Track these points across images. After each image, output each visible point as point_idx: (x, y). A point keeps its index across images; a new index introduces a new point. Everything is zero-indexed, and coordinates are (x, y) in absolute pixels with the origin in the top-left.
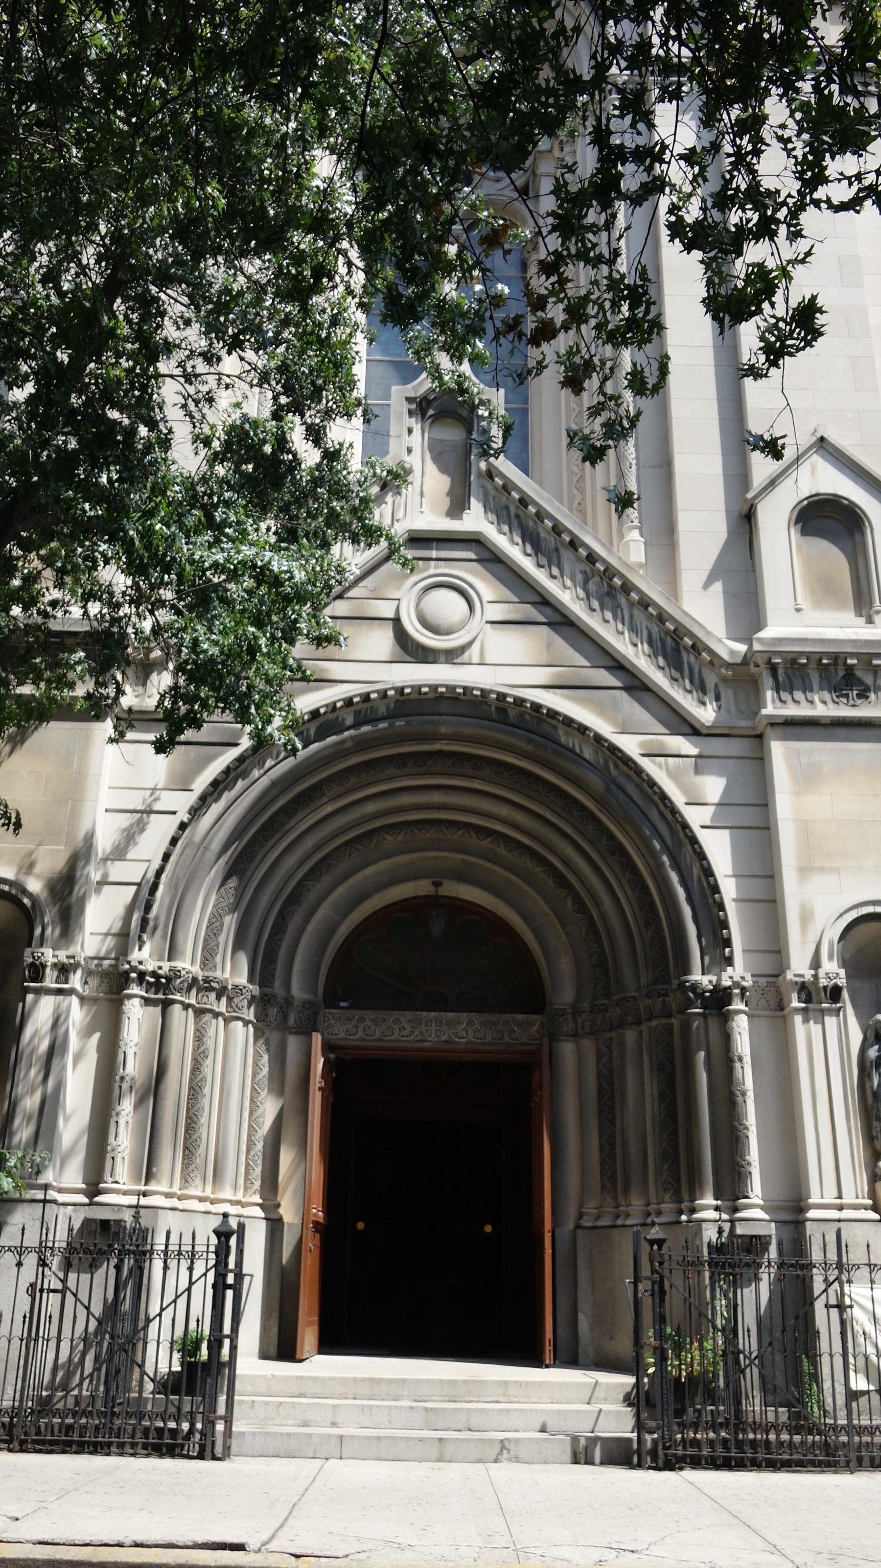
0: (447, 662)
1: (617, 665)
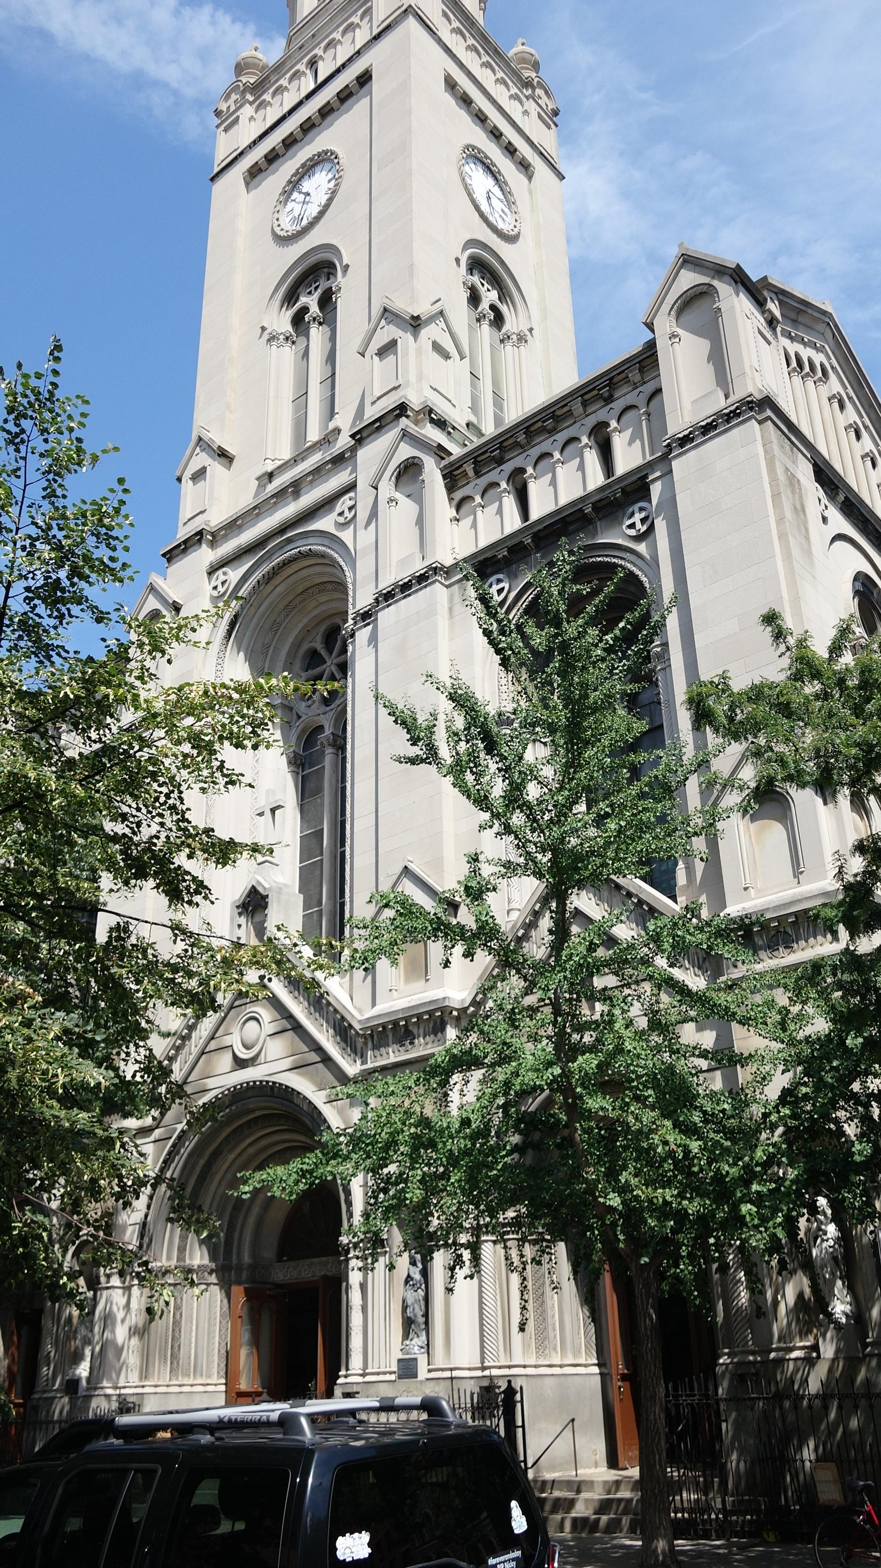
0: (253, 1065)
1: (318, 1049)
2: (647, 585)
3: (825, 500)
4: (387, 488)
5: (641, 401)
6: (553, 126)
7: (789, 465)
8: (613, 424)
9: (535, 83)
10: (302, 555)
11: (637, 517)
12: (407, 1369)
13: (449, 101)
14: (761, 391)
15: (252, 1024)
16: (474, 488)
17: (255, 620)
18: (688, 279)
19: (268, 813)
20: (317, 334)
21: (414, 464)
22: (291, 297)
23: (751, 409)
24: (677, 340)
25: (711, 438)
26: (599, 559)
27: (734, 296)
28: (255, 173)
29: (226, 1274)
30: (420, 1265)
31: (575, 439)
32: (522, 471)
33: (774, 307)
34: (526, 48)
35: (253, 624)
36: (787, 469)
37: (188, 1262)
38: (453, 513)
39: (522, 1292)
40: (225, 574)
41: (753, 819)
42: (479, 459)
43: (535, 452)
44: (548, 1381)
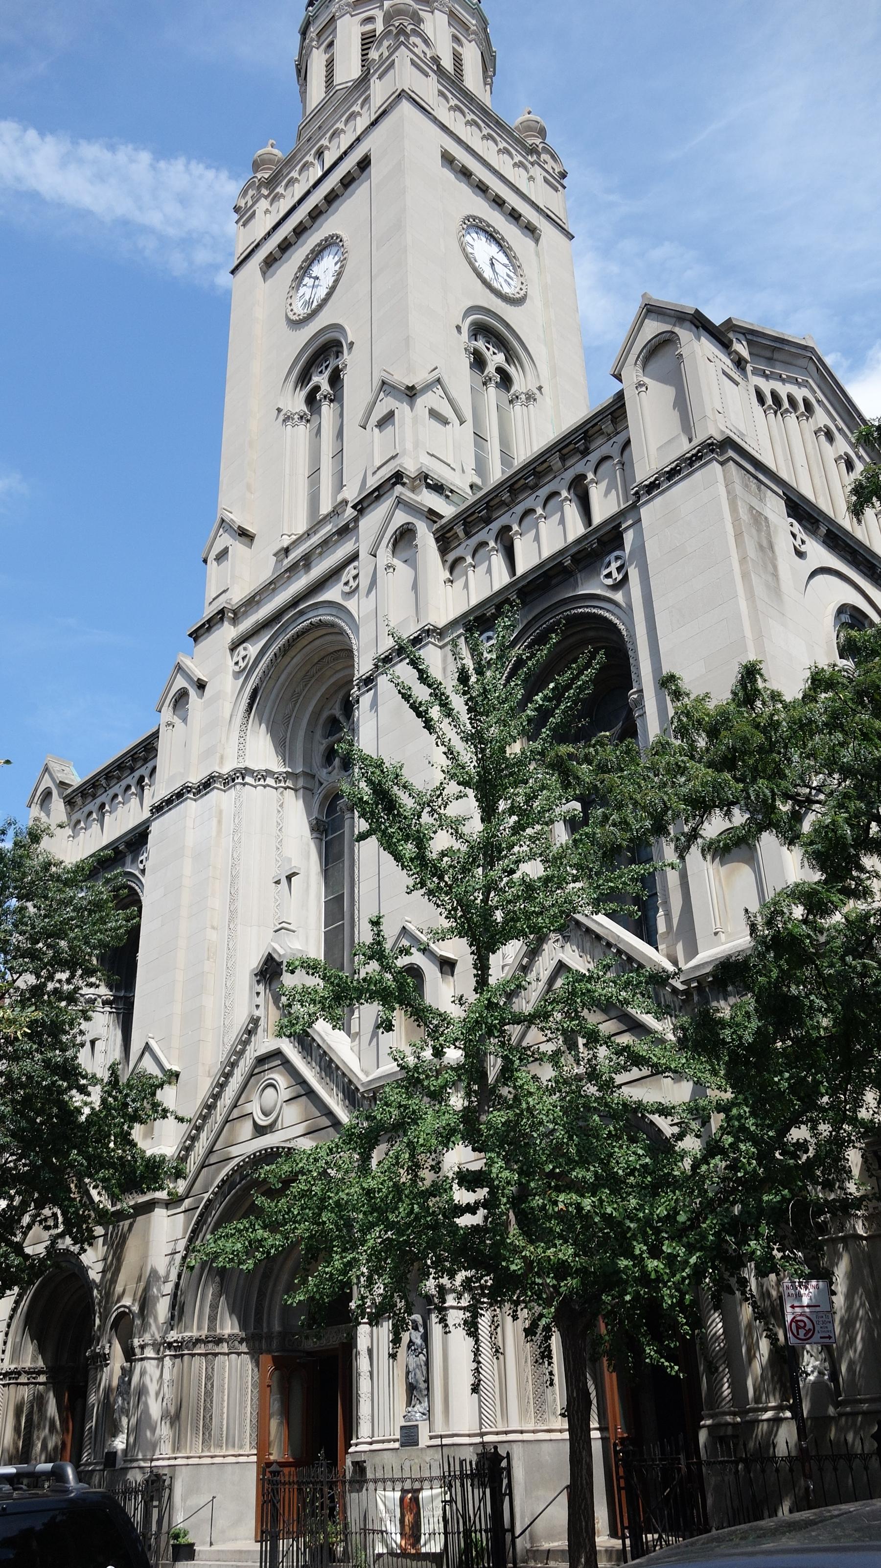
2: (624, 633)
3: (802, 535)
4: (385, 555)
5: (615, 451)
6: (560, 188)
7: (755, 503)
8: (590, 476)
9: (540, 149)
10: (313, 627)
11: (614, 566)
12: (409, 1436)
13: (448, 175)
14: (723, 432)
15: (270, 1090)
16: (464, 550)
17: (275, 691)
18: (653, 328)
19: (284, 881)
20: (327, 410)
21: (411, 530)
22: (304, 378)
23: (712, 451)
24: (644, 389)
25: (676, 483)
26: (580, 610)
27: (695, 342)
28: (270, 262)
29: (257, 1343)
30: (421, 1329)
31: (555, 494)
32: (508, 528)
33: (742, 349)
34: (532, 117)
35: (273, 696)
36: (752, 508)
37: (218, 1331)
38: (447, 575)
39: (475, 1355)
40: (245, 649)
41: (722, 863)
42: (469, 520)
43: (519, 509)
44: (546, 1447)
